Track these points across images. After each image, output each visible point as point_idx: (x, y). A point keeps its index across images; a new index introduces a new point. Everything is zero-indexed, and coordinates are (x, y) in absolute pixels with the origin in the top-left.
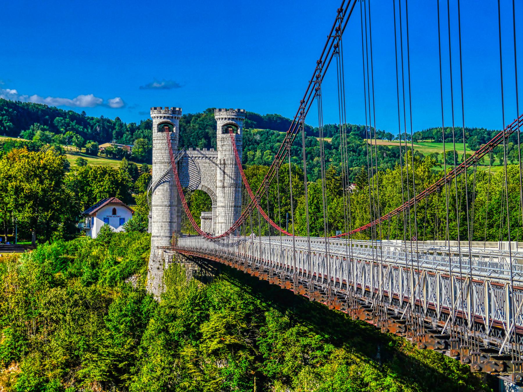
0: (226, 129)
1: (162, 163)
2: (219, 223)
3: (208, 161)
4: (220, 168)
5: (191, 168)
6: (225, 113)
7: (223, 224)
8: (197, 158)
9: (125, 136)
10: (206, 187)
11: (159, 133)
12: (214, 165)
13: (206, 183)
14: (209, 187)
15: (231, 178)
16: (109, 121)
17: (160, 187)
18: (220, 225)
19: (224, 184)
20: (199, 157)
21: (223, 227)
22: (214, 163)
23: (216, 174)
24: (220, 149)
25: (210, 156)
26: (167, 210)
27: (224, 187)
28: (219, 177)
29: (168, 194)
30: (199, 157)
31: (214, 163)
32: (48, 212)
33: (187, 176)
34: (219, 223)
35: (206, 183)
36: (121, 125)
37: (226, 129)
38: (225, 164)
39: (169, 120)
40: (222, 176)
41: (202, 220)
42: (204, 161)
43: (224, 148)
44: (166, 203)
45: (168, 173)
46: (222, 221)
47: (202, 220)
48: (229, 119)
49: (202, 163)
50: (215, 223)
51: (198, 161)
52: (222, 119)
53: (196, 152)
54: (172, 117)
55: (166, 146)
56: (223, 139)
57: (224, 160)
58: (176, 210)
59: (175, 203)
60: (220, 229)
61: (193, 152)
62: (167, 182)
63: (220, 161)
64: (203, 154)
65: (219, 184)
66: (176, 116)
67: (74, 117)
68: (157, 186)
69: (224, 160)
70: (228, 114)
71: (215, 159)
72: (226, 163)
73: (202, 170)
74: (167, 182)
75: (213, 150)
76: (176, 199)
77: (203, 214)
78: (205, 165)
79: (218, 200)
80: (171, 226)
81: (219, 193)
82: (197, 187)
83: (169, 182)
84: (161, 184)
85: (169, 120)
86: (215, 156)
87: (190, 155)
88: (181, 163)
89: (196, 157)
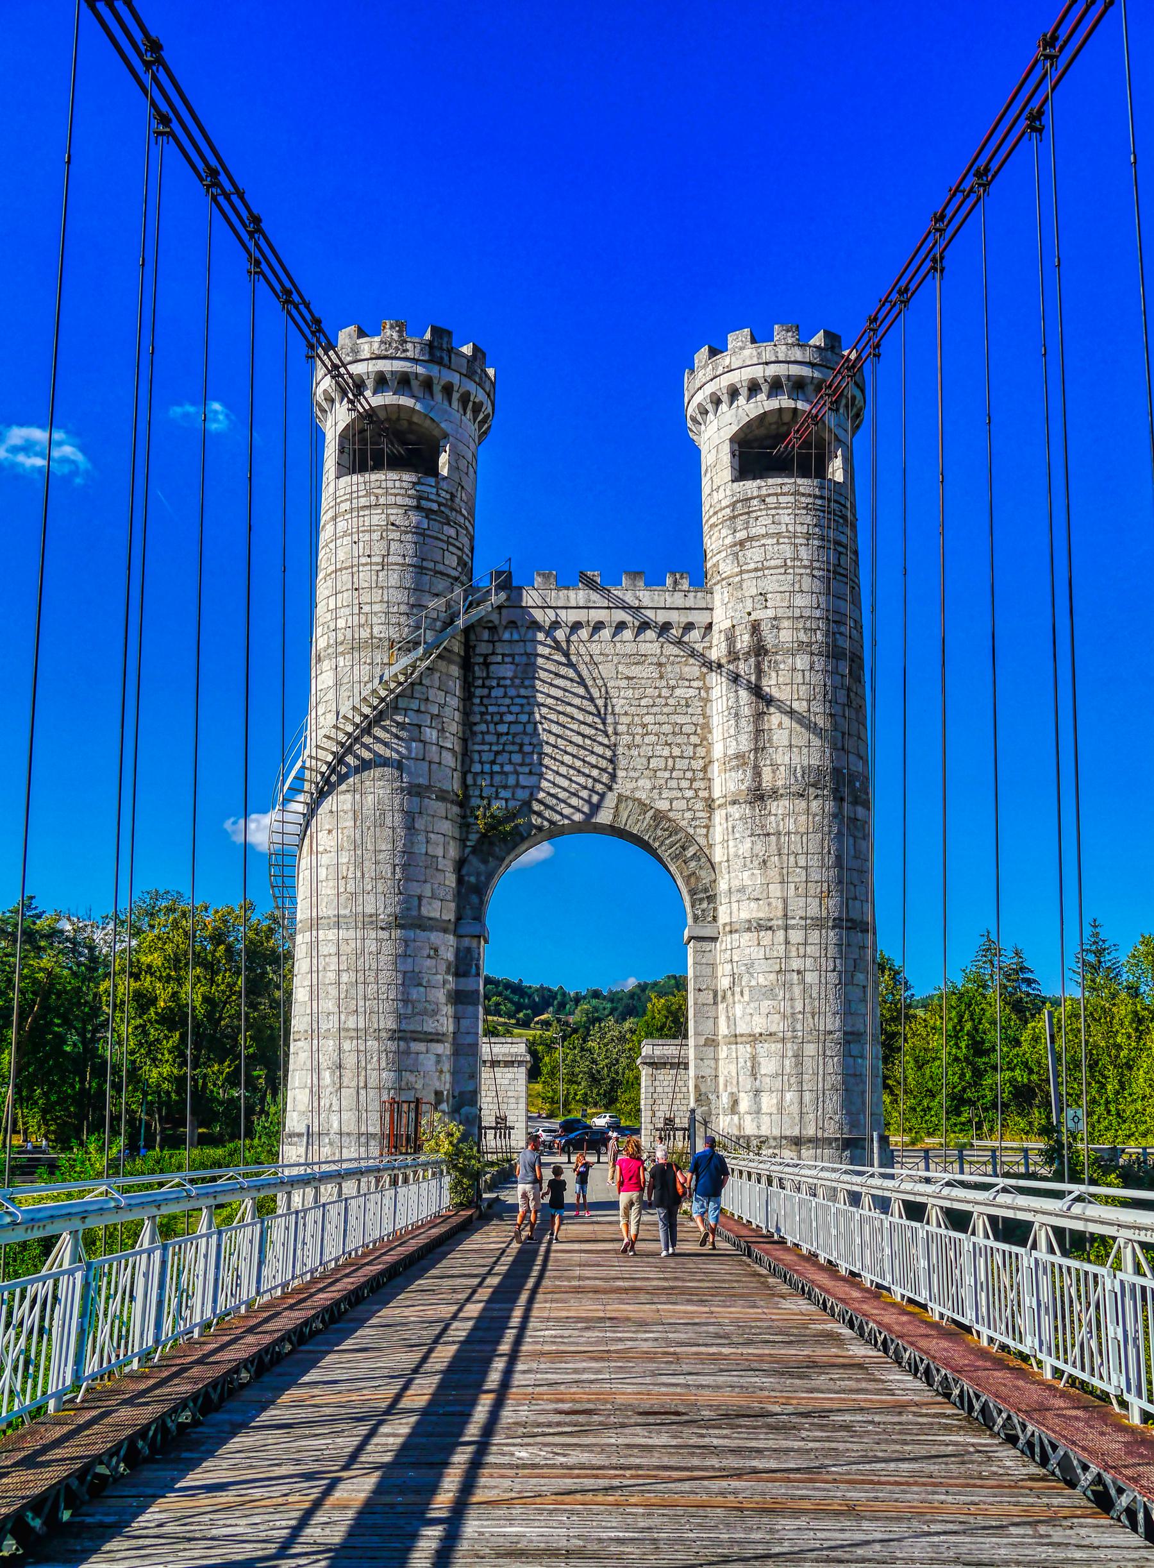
0: (756, 454)
1: (356, 647)
2: (735, 1039)
3: (650, 644)
4: (735, 679)
5: (550, 687)
6: (750, 352)
7: (762, 1049)
8: (584, 633)
9: (568, 1007)
10: (644, 807)
11: (346, 479)
12: (693, 669)
13: (645, 783)
14: (663, 805)
15: (811, 727)
16: (550, 990)
17: (341, 801)
18: (744, 1051)
19: (757, 774)
20: (599, 626)
21: (768, 1067)
22: (693, 654)
23: (707, 727)
24: (727, 568)
25: (662, 617)
26: (380, 947)
27: (758, 796)
28: (725, 737)
29: (384, 845)
30: (599, 626)
31: (693, 654)
32: (221, 1062)
33: (526, 747)
34: (735, 1039)
35: (648, 784)
36: (564, 994)
37: (756, 454)
38: (759, 650)
39: (406, 401)
40: (747, 727)
41: (643, 1073)
42: (630, 648)
43: (753, 555)
44: (379, 903)
45: (394, 707)
46: (759, 1025)
47: (645, 1072)
48: (776, 387)
49: (618, 663)
50: (712, 1042)
51: (595, 648)
52: (734, 393)
53: (579, 596)
54: (428, 384)
55: (379, 548)
56: (741, 509)
57: (755, 628)
58: (450, 956)
59: (441, 909)
60: (746, 1082)
61: (558, 597)
62: (385, 762)
63: (731, 639)
64: (626, 607)
65: (726, 783)
66: (455, 378)
67: (508, 985)
68: (322, 795)
69: (755, 628)
70: (768, 355)
71: (695, 635)
72: (769, 640)
73: (619, 705)
74: (385, 762)
75: (685, 584)
76: (451, 880)
77: (646, 1050)
78: (635, 671)
79: (723, 886)
80: (403, 1063)
81: (729, 842)
82: (595, 808)
83: (399, 766)
84: (343, 778)
85: (406, 401)
86: (693, 617)
87: (538, 615)
88: (486, 664)
89: (576, 626)
